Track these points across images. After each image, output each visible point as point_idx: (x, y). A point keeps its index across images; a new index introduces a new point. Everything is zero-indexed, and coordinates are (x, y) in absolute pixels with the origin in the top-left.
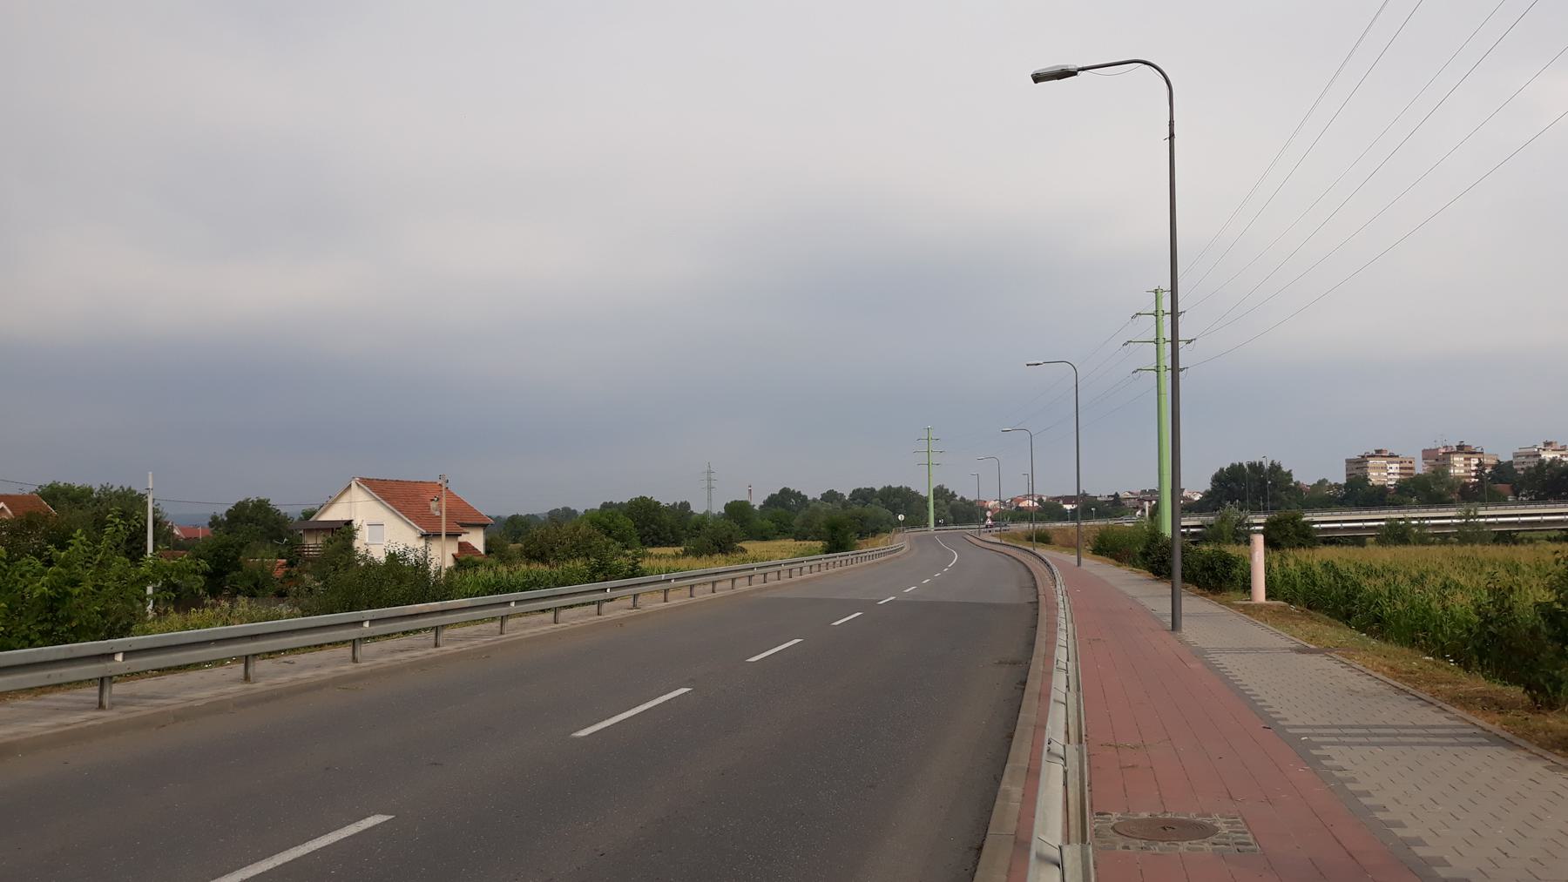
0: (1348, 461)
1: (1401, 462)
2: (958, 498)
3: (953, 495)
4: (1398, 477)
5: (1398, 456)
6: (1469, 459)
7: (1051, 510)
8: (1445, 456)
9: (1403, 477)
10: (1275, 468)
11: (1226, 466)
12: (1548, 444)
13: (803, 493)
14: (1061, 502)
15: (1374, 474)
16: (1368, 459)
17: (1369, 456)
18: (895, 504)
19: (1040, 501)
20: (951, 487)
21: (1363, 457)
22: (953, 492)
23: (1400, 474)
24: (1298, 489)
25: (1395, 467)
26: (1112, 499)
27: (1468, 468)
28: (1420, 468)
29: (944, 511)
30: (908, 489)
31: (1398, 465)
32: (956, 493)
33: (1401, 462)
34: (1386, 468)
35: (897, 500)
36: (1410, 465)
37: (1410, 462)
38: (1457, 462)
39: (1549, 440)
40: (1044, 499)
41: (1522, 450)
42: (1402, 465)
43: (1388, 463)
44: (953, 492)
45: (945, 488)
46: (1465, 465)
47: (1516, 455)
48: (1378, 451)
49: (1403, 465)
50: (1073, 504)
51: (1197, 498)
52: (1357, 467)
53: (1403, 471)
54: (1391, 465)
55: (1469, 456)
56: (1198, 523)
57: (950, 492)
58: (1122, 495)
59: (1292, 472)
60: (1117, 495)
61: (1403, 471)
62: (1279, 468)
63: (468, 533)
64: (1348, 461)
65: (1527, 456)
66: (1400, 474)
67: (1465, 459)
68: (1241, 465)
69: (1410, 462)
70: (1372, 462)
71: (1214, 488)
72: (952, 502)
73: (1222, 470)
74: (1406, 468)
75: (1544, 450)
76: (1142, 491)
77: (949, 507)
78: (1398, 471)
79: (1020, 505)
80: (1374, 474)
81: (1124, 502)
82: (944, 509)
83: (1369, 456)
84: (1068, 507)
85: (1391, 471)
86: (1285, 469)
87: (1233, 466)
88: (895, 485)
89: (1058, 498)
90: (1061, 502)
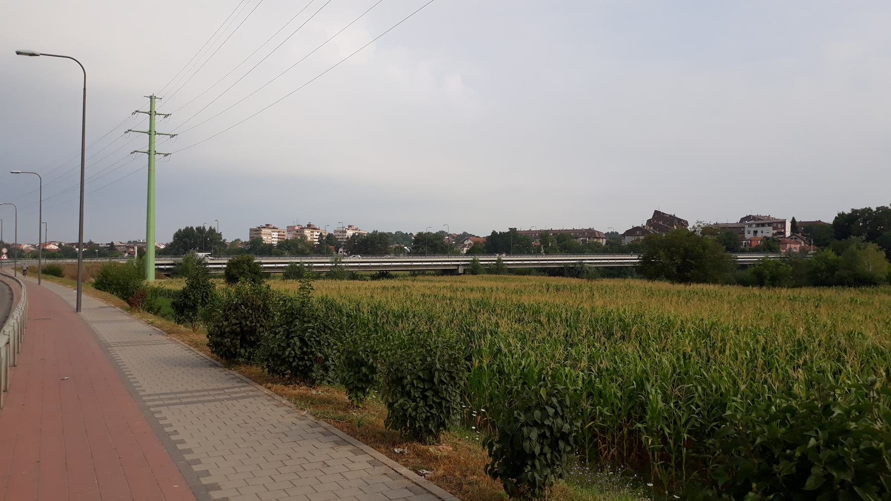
0: (251, 230)
1: (279, 232)
4: (277, 240)
5: (277, 229)
6: (313, 232)
7: (66, 251)
8: (302, 229)
9: (280, 240)
10: (212, 231)
11: (183, 228)
12: (350, 226)
14: (75, 247)
15: (265, 238)
16: (262, 229)
17: (262, 228)
19: (60, 245)
21: (259, 228)
23: (278, 238)
24: (224, 244)
25: (275, 235)
26: (109, 246)
27: (312, 237)
28: (289, 236)
31: (277, 233)
33: (279, 232)
34: (271, 234)
36: (283, 234)
37: (284, 232)
38: (308, 233)
39: (351, 225)
40: (63, 244)
41: (339, 229)
42: (279, 233)
43: (272, 232)
46: (311, 235)
47: (335, 231)
48: (267, 225)
49: (280, 233)
51: (162, 247)
52: (256, 232)
53: (280, 237)
54: (274, 233)
55: (312, 230)
56: (171, 262)
58: (115, 244)
59: (222, 234)
60: (112, 243)
61: (280, 237)
62: (214, 230)
63: (107, 244)
64: (251, 230)
65: (341, 232)
66: (278, 238)
67: (311, 232)
68: (192, 228)
69: (284, 232)
70: (264, 231)
71: (175, 241)
73: (180, 230)
74: (281, 235)
75: (348, 229)
78: (277, 237)
80: (265, 238)
81: (117, 248)
83: (262, 228)
85: (273, 236)
86: (218, 231)
87: (187, 228)
90: (75, 247)
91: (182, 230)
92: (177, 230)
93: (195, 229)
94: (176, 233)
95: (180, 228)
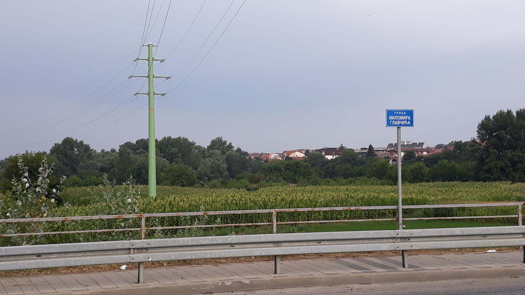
2: (235, 149)
3: (230, 147)
13: (85, 143)
14: (323, 153)
18: (172, 154)
20: (228, 139)
22: (230, 144)
29: (219, 161)
30: (186, 140)
32: (233, 145)
35: (175, 150)
44: (230, 144)
45: (224, 140)
50: (333, 155)
57: (228, 144)
60: (371, 147)
72: (228, 152)
76: (389, 144)
77: (224, 156)
79: (291, 156)
81: (377, 153)
82: (218, 157)
84: (329, 157)
88: (174, 136)
89: (321, 151)
90: (323, 153)
91: (491, 118)
92: (483, 118)
93: (515, 114)
94: (482, 122)
95: (487, 114)
